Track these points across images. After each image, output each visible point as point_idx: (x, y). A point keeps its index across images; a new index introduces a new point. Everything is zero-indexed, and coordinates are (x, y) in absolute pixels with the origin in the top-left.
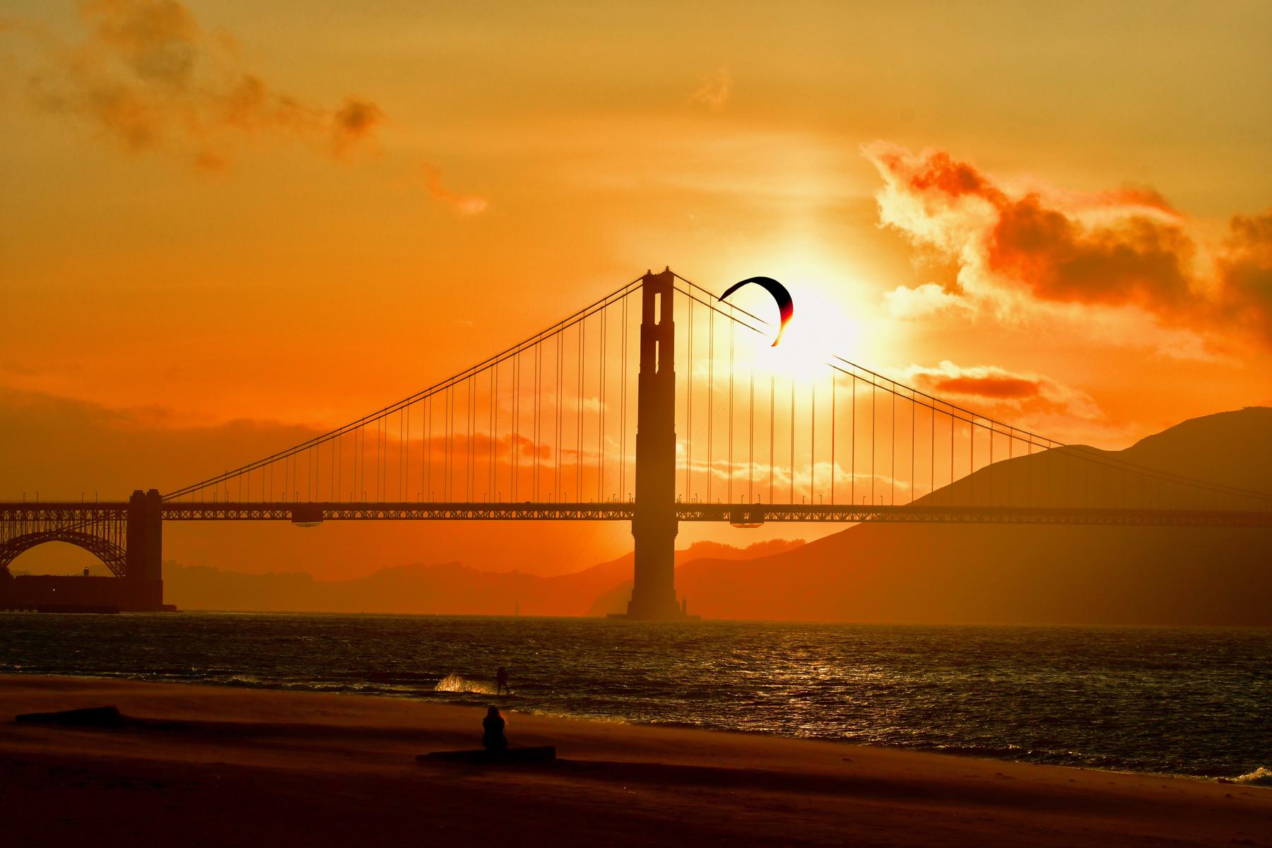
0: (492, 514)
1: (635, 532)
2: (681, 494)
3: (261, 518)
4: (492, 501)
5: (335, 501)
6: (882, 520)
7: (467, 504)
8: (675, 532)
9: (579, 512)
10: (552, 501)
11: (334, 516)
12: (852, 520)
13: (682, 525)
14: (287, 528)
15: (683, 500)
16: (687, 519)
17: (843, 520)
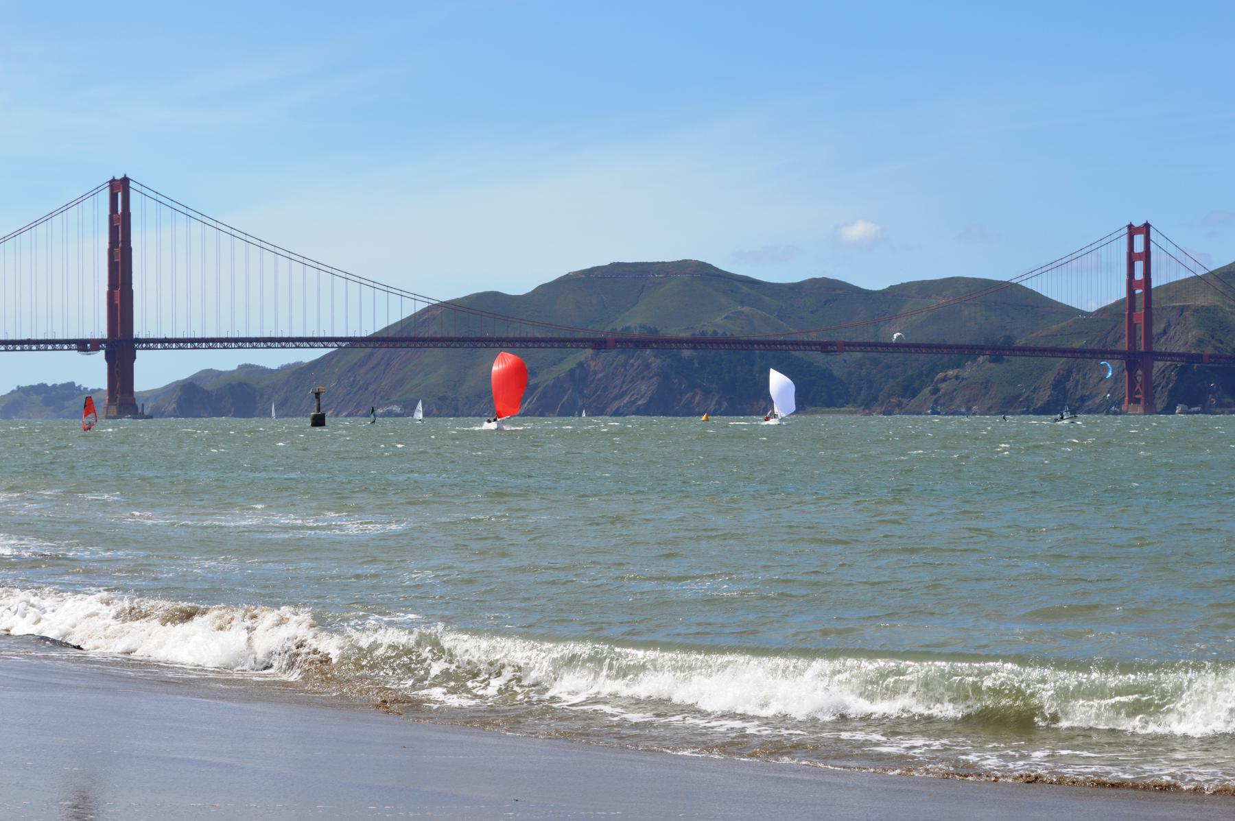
0: (174, 345)
1: (108, 358)
2: (139, 331)
3: (46, 350)
4: (189, 337)
5: (65, 338)
6: (353, 347)
7: (202, 339)
8: (134, 358)
9: (218, 344)
10: (185, 337)
11: (17, 349)
12: (332, 347)
13: (140, 354)
14: (75, 355)
15: (140, 337)
16: (143, 349)
17: (325, 347)
